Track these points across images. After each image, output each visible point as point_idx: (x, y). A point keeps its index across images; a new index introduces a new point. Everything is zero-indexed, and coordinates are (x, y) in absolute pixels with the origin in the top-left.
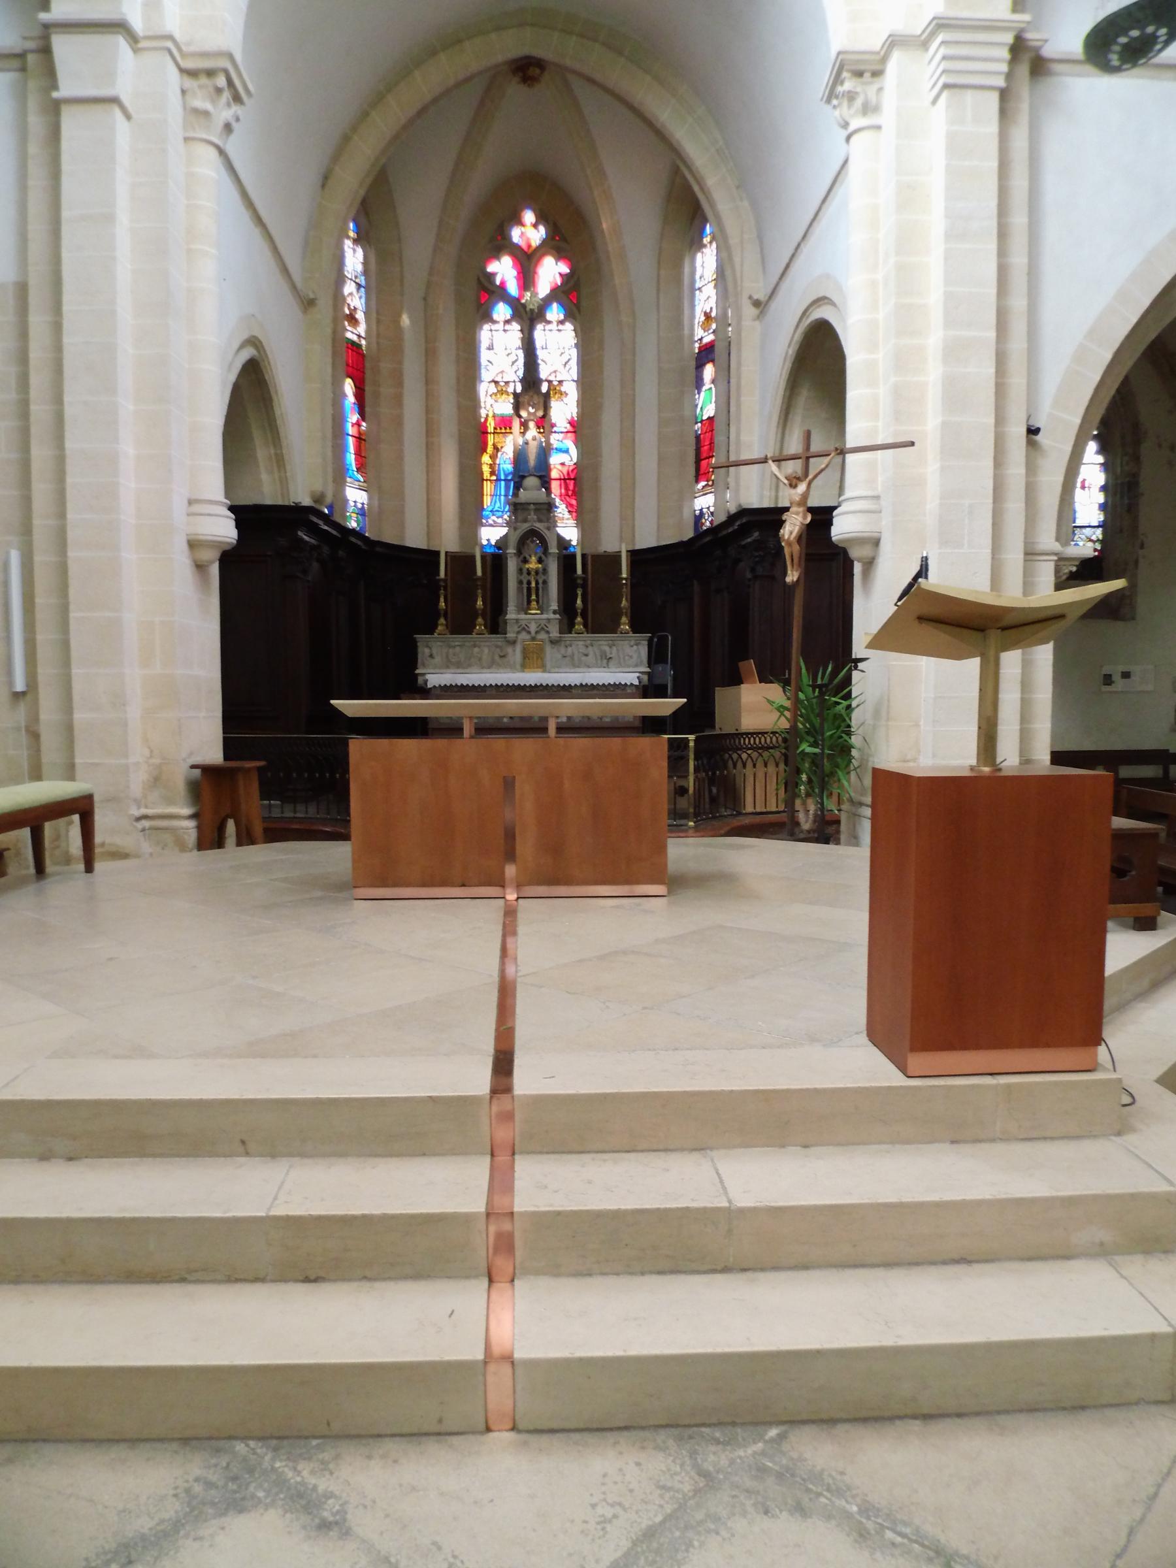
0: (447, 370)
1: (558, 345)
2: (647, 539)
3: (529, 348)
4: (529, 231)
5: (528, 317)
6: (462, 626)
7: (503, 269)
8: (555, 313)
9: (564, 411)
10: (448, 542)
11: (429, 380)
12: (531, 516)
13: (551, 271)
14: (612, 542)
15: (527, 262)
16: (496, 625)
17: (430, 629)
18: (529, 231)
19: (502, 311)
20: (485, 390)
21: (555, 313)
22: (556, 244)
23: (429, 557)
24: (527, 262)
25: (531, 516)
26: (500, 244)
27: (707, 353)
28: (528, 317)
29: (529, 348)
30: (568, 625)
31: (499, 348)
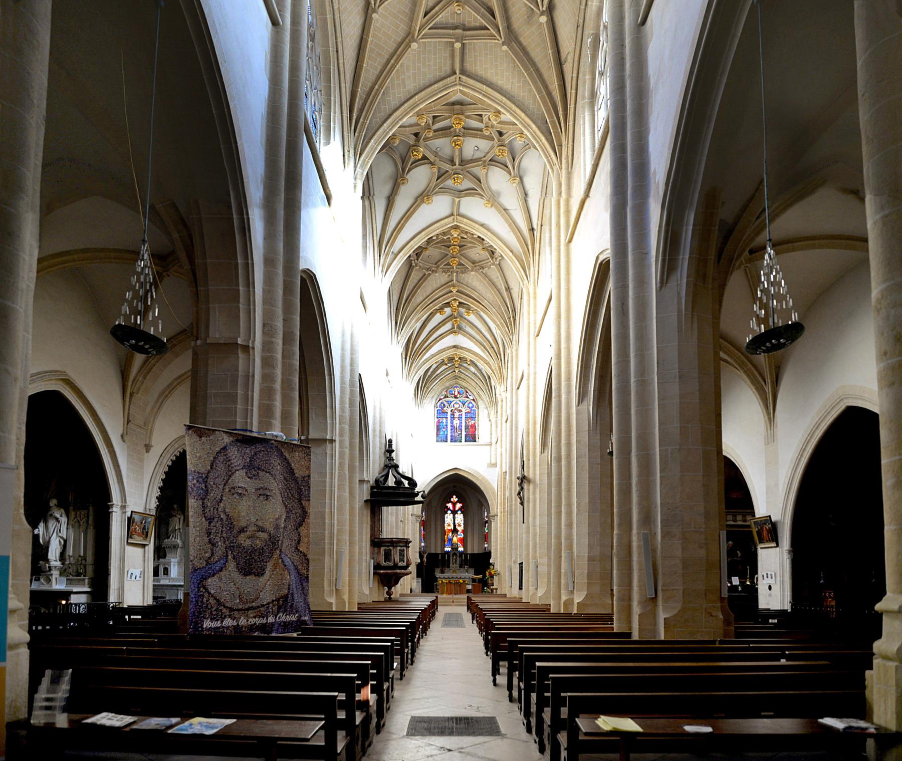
0: (439, 523)
1: (460, 518)
2: (476, 552)
4: (455, 499)
5: (454, 512)
7: (450, 505)
8: (459, 512)
9: (460, 529)
10: (439, 552)
11: (436, 525)
13: (458, 506)
14: (469, 552)
15: (454, 504)
18: (455, 499)
19: (449, 512)
20: (446, 525)
21: (459, 512)
23: (436, 555)
24: (454, 504)
27: (486, 522)
28: (454, 512)
30: (461, 566)
31: (449, 518)
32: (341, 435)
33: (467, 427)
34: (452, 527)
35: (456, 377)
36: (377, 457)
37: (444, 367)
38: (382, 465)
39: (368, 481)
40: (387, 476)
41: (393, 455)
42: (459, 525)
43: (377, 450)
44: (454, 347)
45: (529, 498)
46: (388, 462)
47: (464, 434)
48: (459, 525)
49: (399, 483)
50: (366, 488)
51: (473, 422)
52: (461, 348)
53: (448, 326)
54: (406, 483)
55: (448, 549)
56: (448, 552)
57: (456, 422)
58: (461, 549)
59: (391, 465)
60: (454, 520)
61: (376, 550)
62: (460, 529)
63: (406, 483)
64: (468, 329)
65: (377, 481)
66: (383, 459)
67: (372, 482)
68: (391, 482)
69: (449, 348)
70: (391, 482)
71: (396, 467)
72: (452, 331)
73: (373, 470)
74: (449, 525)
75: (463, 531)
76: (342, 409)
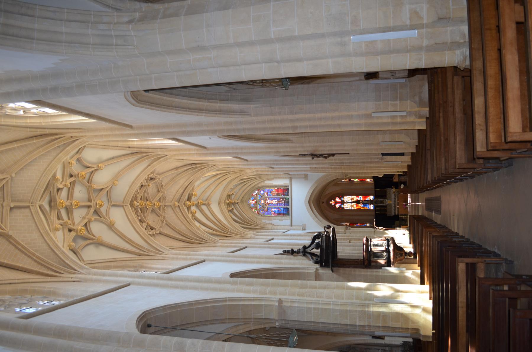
1: (347, 199)
3: (347, 202)
4: (332, 202)
5: (343, 202)
6: (386, 211)
8: (343, 199)
9: (355, 198)
10: (373, 213)
12: (371, 202)
13: (338, 200)
14: (374, 192)
15: (336, 203)
16: (386, 207)
17: (386, 214)
18: (332, 202)
19: (342, 206)
21: (343, 199)
22: (334, 199)
24: (336, 203)
25: (371, 202)
26: (334, 206)
27: (350, 180)
28: (343, 202)
29: (347, 202)
31: (347, 206)
32: (275, 293)
33: (278, 195)
34: (354, 204)
35: (242, 201)
36: (297, 261)
37: (235, 210)
38: (304, 258)
39: (317, 269)
40: (312, 254)
41: (295, 250)
42: (353, 199)
43: (292, 261)
44: (219, 204)
45: (329, 150)
46: (301, 254)
47: (283, 196)
48: (353, 199)
49: (318, 246)
50: (321, 271)
51: (274, 191)
52: (220, 199)
53: (204, 208)
54: (317, 241)
55: (372, 207)
56: (375, 207)
57: (274, 202)
58: (371, 198)
59: (304, 251)
60: (349, 202)
61: (373, 264)
62: (355, 198)
63: (317, 241)
64: (207, 195)
65: (316, 262)
66: (299, 257)
67: (317, 266)
68: (317, 251)
69: (220, 207)
70: (317, 251)
71: (305, 248)
72: (208, 205)
73: (307, 265)
74: (353, 206)
75: (358, 196)
76: (255, 292)
